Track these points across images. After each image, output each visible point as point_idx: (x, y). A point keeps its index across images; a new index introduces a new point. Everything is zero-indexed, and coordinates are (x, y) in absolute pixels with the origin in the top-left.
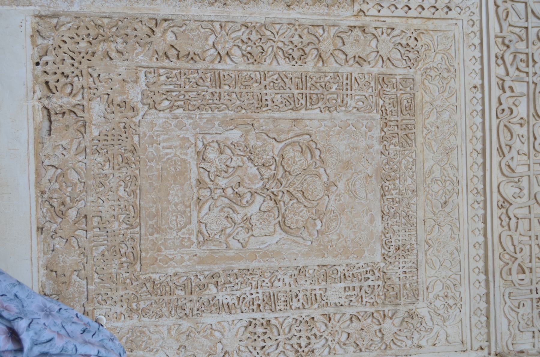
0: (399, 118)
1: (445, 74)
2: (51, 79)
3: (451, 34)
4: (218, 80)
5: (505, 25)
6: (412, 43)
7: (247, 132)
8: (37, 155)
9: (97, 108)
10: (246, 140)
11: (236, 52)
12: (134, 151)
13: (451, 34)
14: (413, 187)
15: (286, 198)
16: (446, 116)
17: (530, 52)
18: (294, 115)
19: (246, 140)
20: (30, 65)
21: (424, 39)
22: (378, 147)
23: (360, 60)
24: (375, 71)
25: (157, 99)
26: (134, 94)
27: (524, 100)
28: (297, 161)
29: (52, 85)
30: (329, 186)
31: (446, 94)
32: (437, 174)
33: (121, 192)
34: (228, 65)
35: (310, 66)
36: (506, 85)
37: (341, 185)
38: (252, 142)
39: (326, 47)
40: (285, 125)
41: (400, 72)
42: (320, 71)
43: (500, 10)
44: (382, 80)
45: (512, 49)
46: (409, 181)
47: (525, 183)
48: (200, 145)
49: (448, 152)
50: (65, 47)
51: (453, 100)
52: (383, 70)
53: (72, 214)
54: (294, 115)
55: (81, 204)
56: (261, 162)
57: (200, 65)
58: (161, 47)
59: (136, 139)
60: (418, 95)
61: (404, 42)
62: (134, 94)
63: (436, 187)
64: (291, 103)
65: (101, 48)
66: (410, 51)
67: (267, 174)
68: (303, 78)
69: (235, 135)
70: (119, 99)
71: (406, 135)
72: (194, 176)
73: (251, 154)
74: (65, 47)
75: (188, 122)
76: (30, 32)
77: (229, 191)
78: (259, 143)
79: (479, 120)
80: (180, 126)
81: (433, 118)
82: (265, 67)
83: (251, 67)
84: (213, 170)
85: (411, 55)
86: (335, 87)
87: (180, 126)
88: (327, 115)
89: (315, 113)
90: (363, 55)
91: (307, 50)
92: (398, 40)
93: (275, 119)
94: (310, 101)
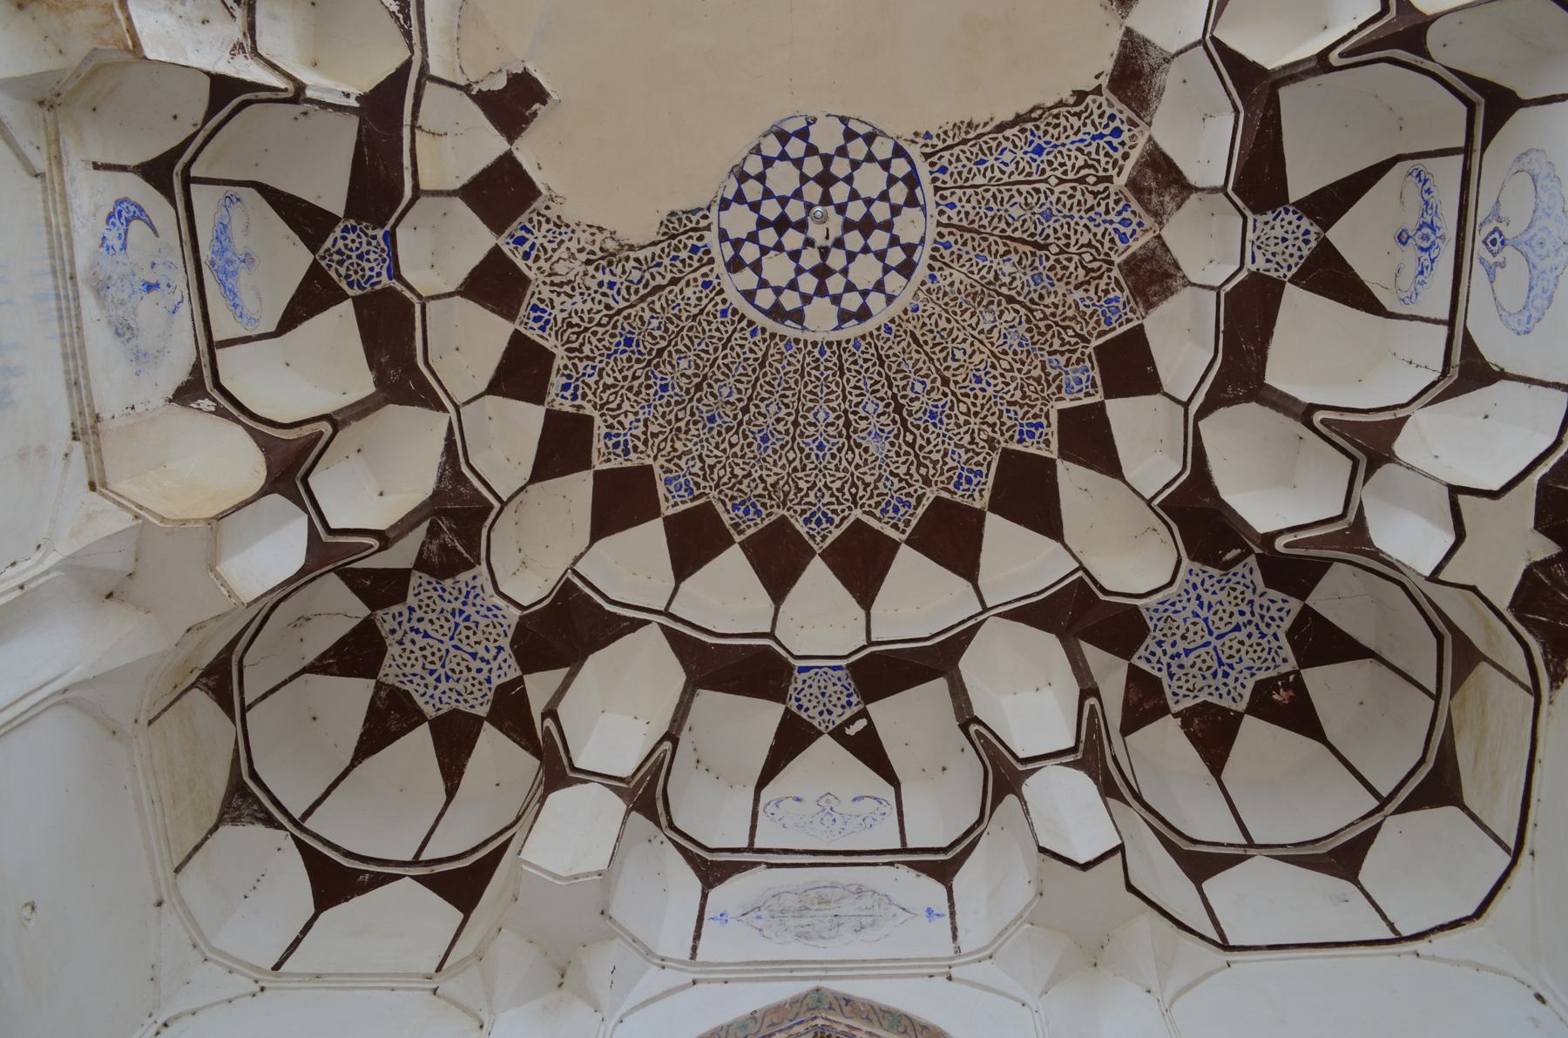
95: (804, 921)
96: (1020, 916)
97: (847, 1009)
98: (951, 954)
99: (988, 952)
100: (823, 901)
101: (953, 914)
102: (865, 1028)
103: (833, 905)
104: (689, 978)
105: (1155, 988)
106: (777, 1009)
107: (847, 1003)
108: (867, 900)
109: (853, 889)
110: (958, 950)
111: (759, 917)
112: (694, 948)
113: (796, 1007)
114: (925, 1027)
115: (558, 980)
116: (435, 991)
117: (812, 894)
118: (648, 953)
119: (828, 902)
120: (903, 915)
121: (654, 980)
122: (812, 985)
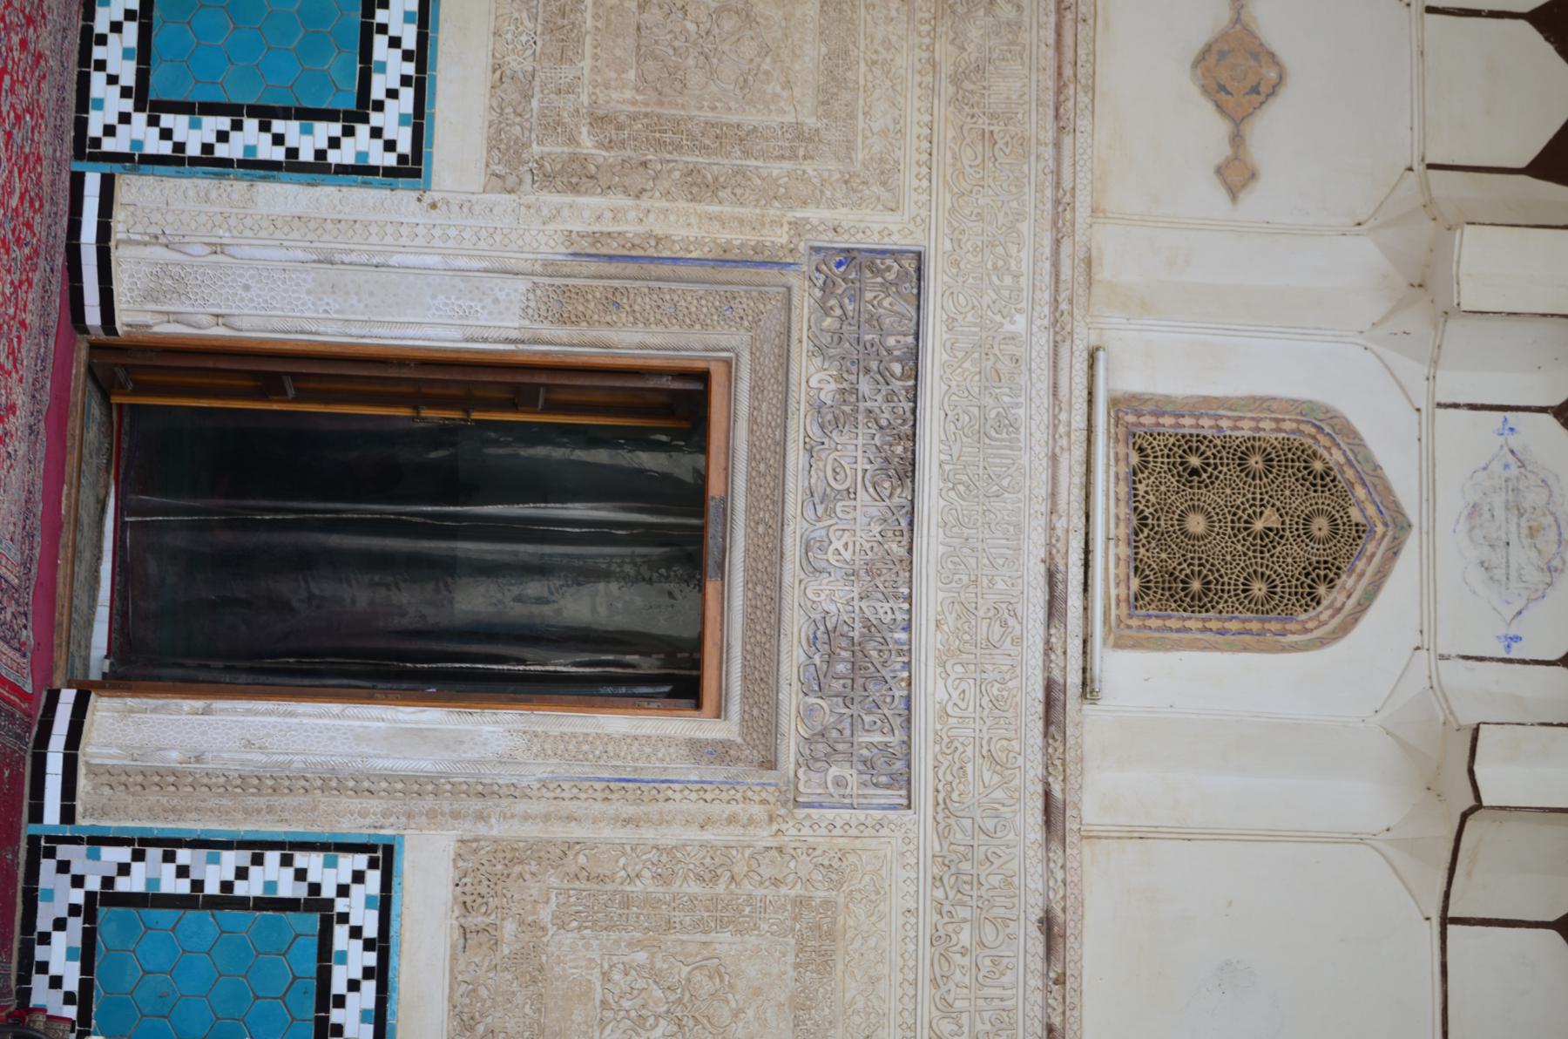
0: (818, 944)
1: (873, 897)
2: (469, 899)
3: (881, 853)
4: (626, 903)
5: (945, 845)
6: (836, 863)
7: (653, 955)
8: (452, 971)
9: (510, 927)
10: (652, 962)
11: (647, 873)
12: (541, 970)
13: (881, 853)
14: (830, 1018)
15: (691, 1023)
16: (872, 942)
17: (974, 872)
18: (703, 938)
19: (652, 962)
20: (451, 886)
21: (852, 858)
22: (792, 974)
23: (776, 882)
24: (793, 893)
25: (566, 919)
26: (545, 914)
27: (967, 926)
28: (706, 986)
29: (469, 904)
30: (736, 1014)
31: (873, 919)
32: (860, 1005)
33: (527, 1010)
34: (638, 886)
35: (721, 889)
36: (944, 910)
37: (750, 1013)
38: (658, 965)
39: (740, 868)
40: (692, 948)
41: (820, 894)
42: (732, 893)
43: (941, 827)
44: (801, 902)
45: (953, 870)
46: (827, 1011)
47: (965, 1019)
48: (606, 966)
49: (874, 981)
50: (483, 869)
51: (882, 925)
52: (802, 892)
53: (480, 1028)
54: (703, 938)
55: (489, 1020)
56: (666, 985)
57: (609, 887)
58: (572, 869)
59: (544, 958)
60: (841, 919)
61: (826, 863)
62: (545, 914)
63: (857, 1019)
64: (700, 926)
65: (517, 869)
66: (834, 872)
67: (672, 997)
68: (715, 899)
69: (641, 957)
70: (530, 919)
71: (825, 961)
72: (598, 997)
73: (656, 976)
74: (483, 869)
75: (595, 943)
76: (452, 855)
77: (633, 1014)
78: (665, 966)
79: (912, 947)
80: (587, 946)
81: (857, 944)
82: (674, 888)
83: (661, 889)
84: (617, 991)
85: (834, 877)
86: (748, 909)
87: (587, 946)
88: (738, 938)
89: (726, 936)
90: (780, 877)
91: (719, 872)
92: (819, 860)
93: (683, 942)
94: (722, 924)
95: (1500, 513)
96: (1451, 713)
97: (1390, 554)
98: (1440, 651)
99: (1435, 685)
100: (1532, 533)
101: (1510, 661)
102: (1370, 570)
103: (1526, 542)
104: (1423, 407)
105: (1389, 835)
106: (1388, 489)
107: (1394, 552)
108: (1534, 577)
109: (1556, 563)
110: (1442, 657)
111: (1506, 466)
112: (1456, 406)
113: (1392, 506)
114: (1356, 620)
115: (1416, 283)
116: (1410, 169)
117: (1549, 520)
118: (1435, 362)
119: (1532, 536)
120: (1509, 612)
121: (1413, 371)
122: (1414, 520)
